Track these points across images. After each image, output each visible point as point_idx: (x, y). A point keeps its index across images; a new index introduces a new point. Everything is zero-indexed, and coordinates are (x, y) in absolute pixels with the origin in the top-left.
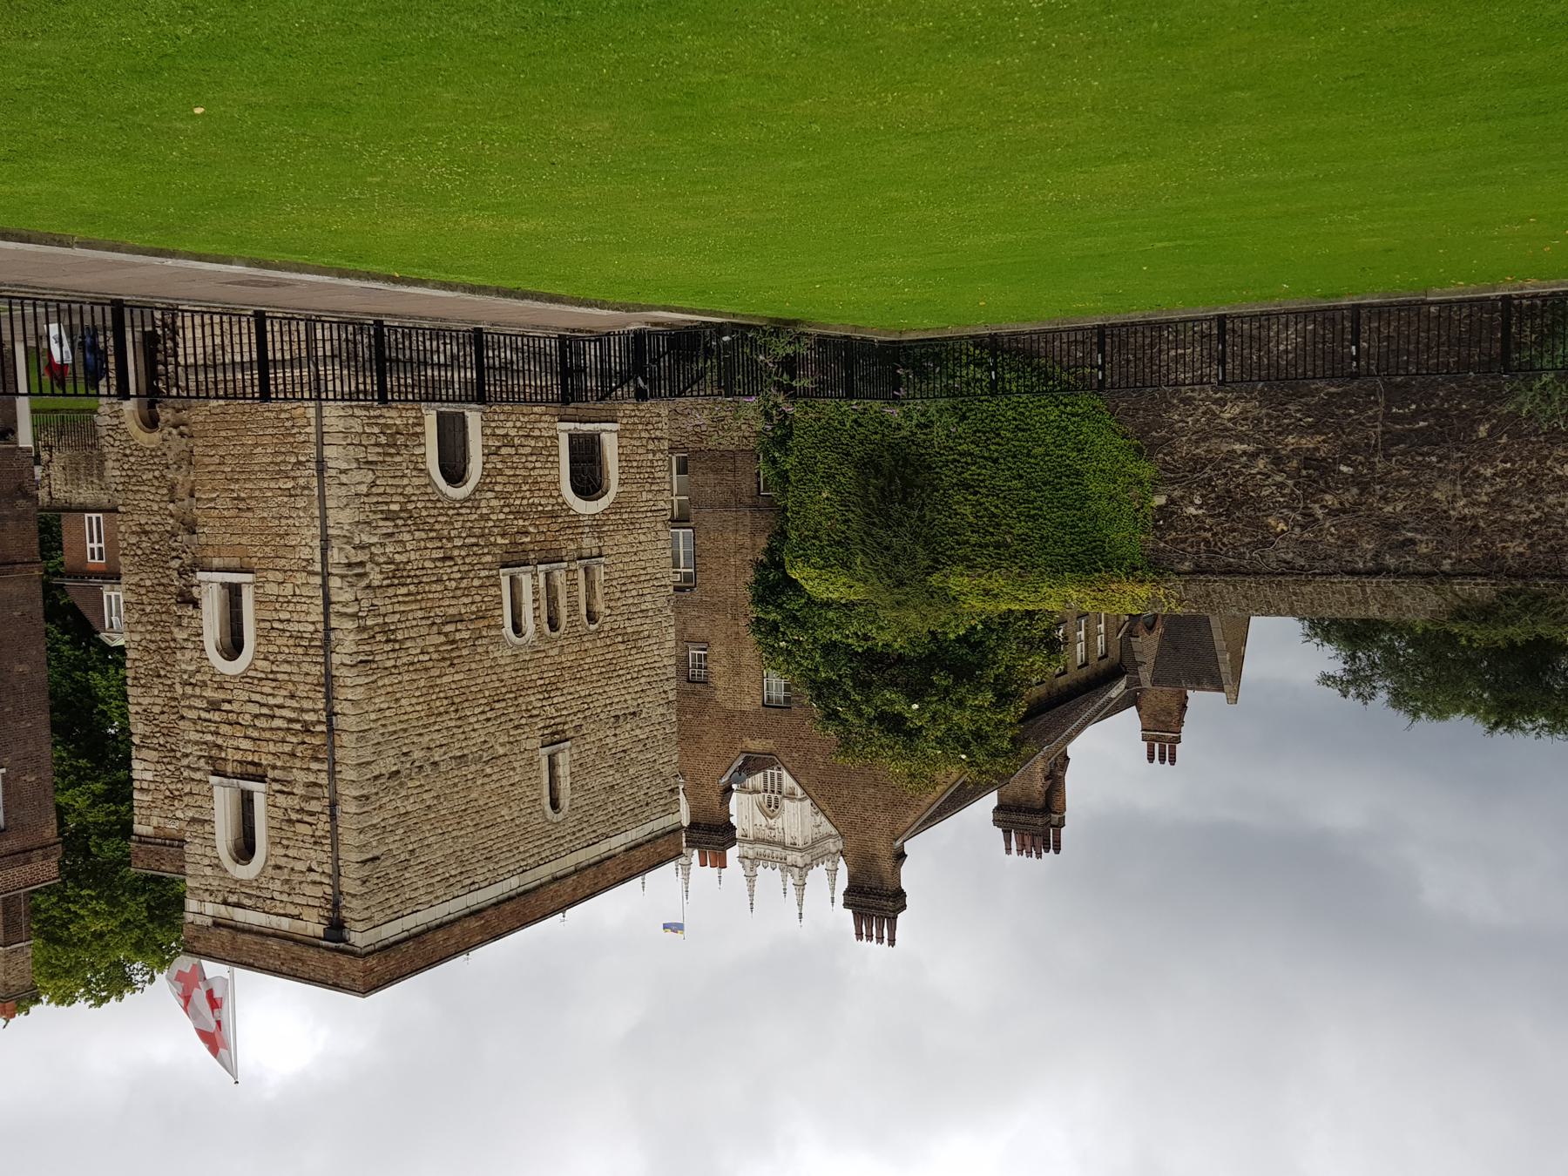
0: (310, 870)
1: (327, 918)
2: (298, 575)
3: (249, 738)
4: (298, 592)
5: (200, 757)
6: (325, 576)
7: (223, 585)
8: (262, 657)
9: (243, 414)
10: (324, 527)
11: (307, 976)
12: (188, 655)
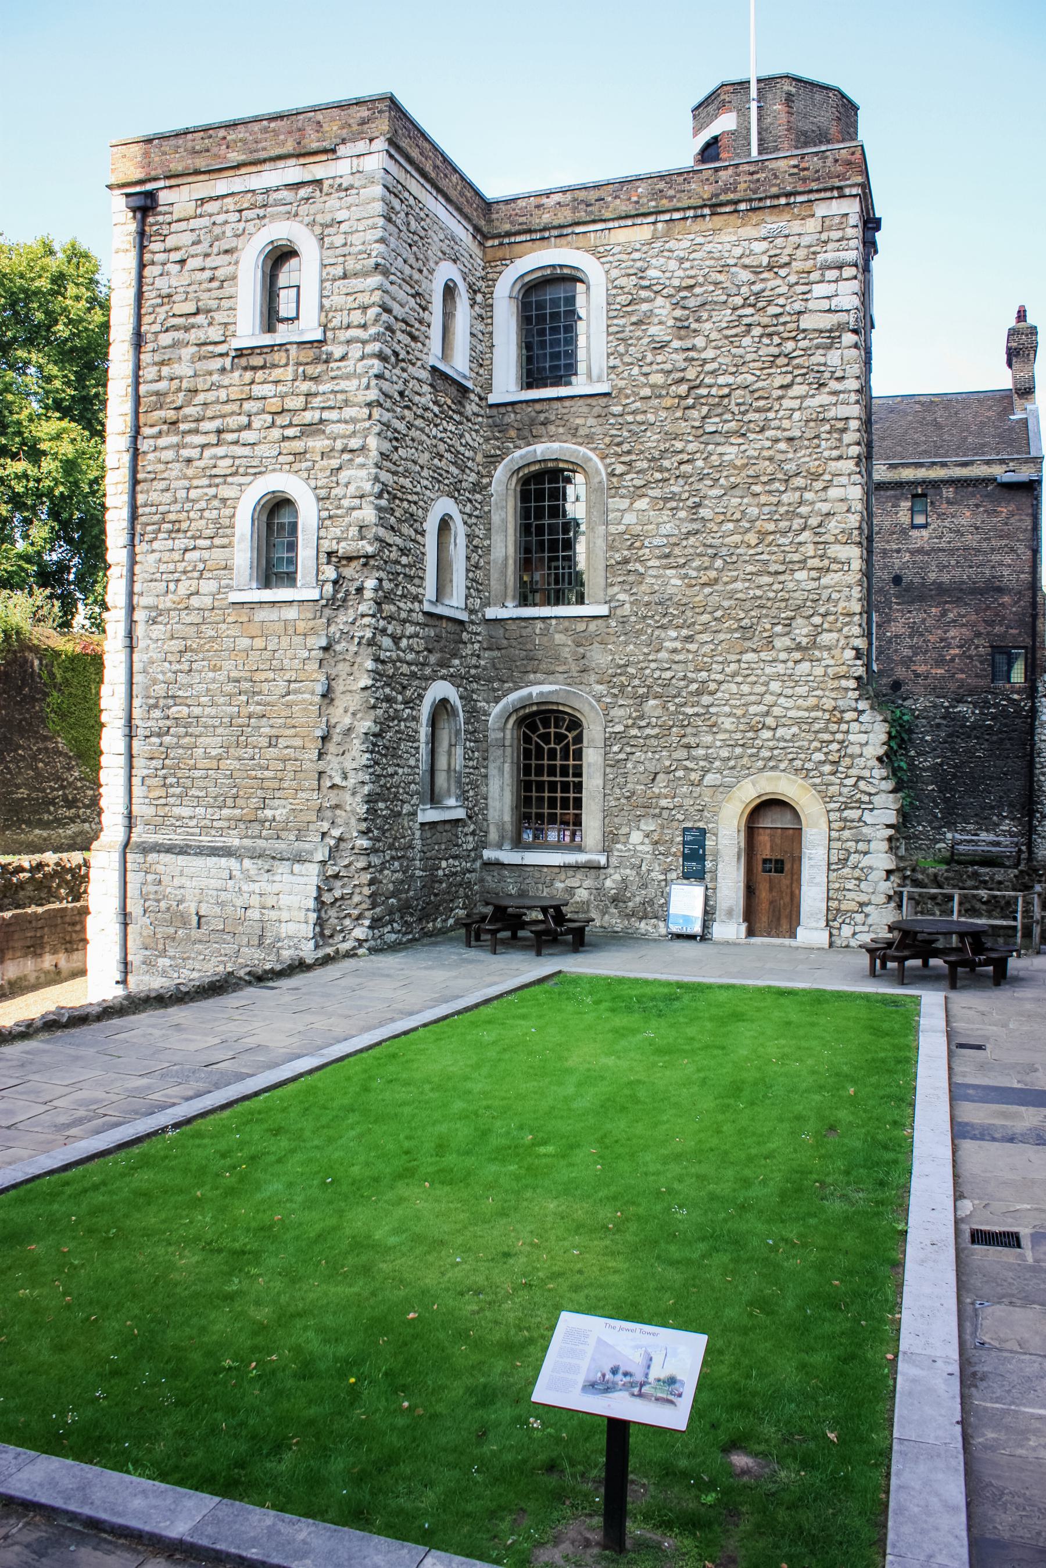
0: (182, 262)
1: (160, 214)
2: (169, 605)
8: (229, 502)
9: (235, 797)
11: (189, 136)
12: (352, 490)
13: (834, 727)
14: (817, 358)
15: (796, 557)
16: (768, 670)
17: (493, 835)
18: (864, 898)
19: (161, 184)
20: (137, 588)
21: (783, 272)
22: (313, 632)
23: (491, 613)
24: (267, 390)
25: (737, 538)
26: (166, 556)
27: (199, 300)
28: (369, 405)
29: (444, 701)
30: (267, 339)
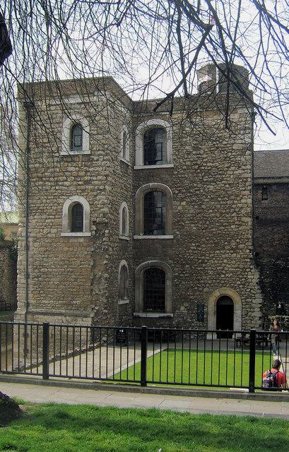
3: (69, 172)
6: (27, 237)
10: (27, 253)
17: (137, 308)
18: (252, 326)
20: (29, 230)
22: (89, 246)
23: (135, 237)
24: (72, 169)
25: (213, 215)
28: (106, 176)
29: (124, 266)
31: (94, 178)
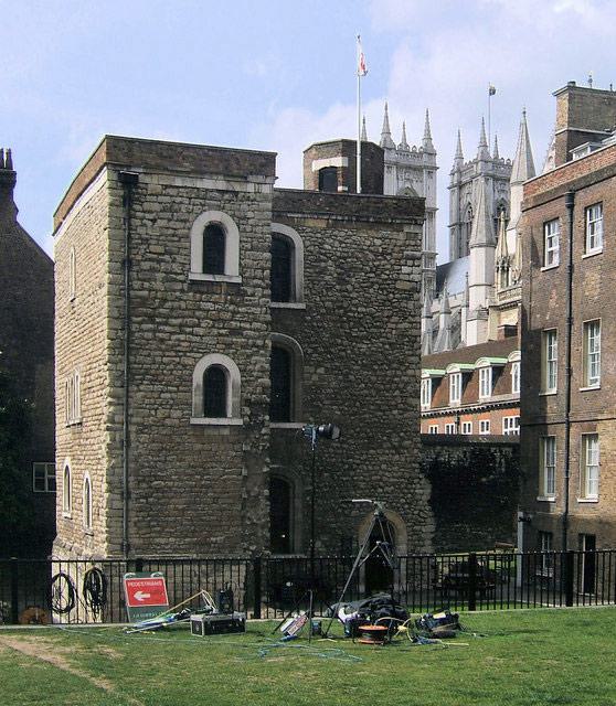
0: (154, 221)
4: (153, 412)
5: (253, 295)
7: (225, 416)
13: (409, 486)
14: (403, 304)
15: (393, 403)
16: (381, 458)
19: (141, 170)
20: (130, 412)
21: (388, 257)
25: (366, 392)
26: (149, 395)
27: (166, 246)
30: (209, 278)
31: (248, 326)
